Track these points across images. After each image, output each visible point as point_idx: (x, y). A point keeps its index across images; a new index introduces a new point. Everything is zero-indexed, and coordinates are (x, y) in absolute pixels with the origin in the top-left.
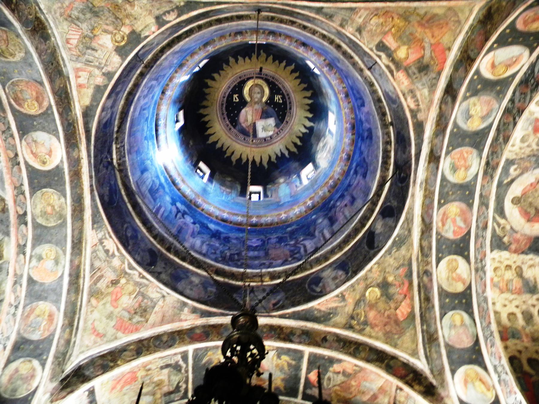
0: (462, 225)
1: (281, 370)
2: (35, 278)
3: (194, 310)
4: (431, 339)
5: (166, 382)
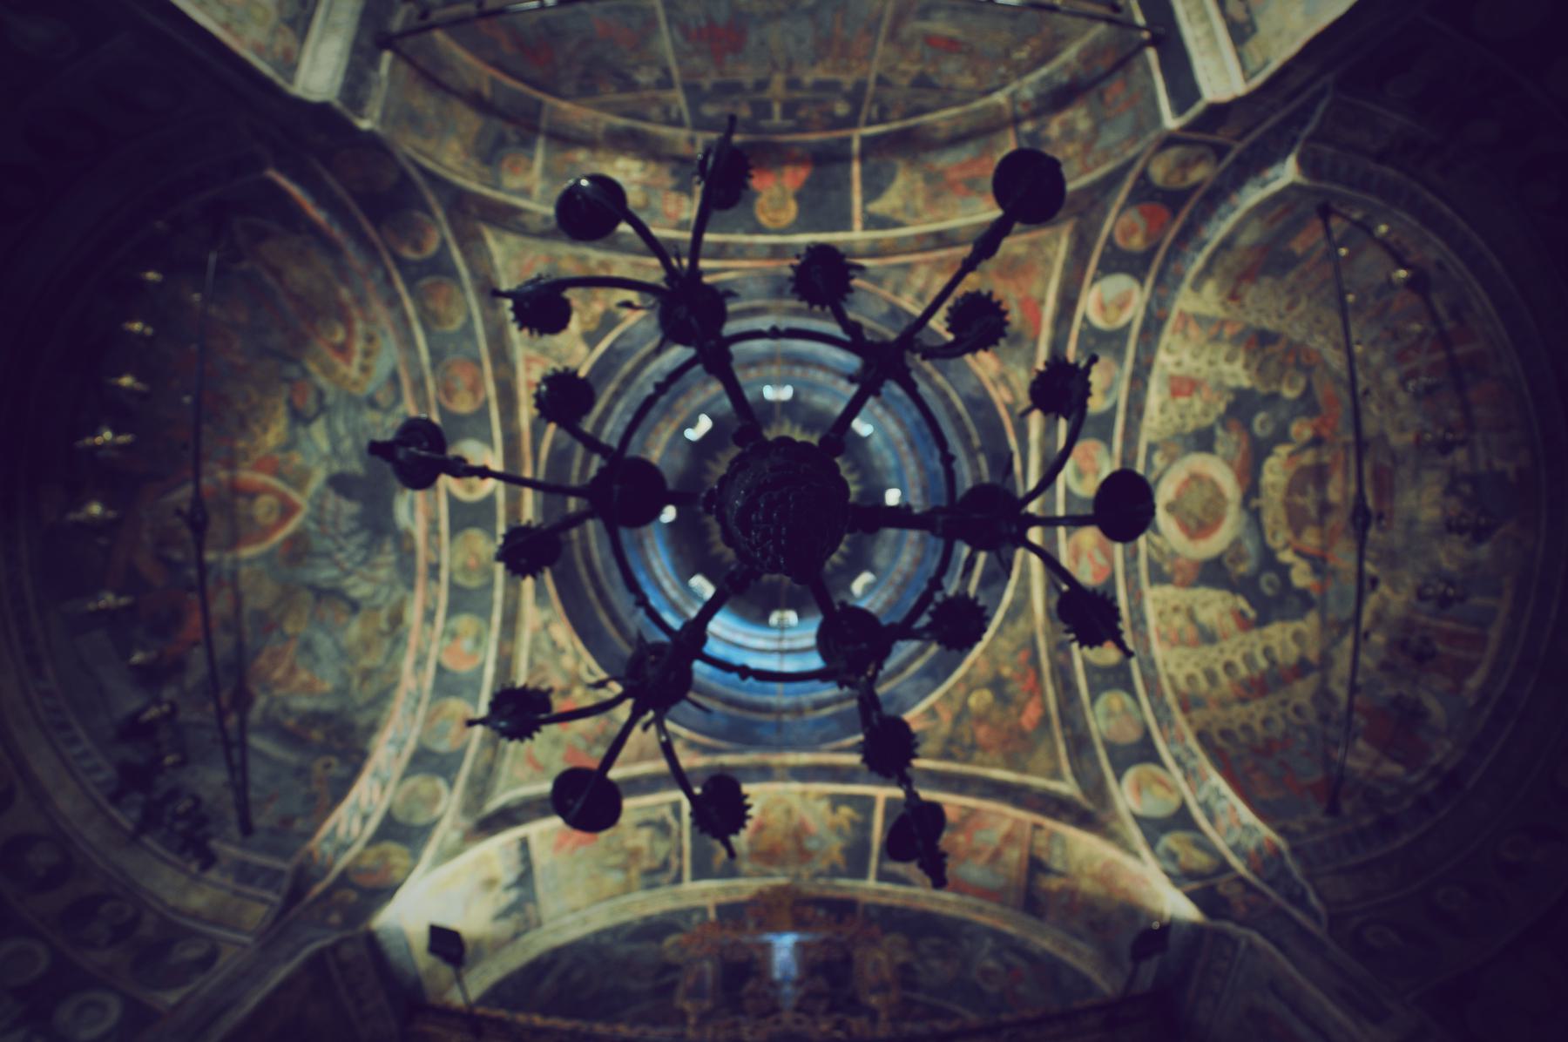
4: (1080, 744)
5: (646, 852)
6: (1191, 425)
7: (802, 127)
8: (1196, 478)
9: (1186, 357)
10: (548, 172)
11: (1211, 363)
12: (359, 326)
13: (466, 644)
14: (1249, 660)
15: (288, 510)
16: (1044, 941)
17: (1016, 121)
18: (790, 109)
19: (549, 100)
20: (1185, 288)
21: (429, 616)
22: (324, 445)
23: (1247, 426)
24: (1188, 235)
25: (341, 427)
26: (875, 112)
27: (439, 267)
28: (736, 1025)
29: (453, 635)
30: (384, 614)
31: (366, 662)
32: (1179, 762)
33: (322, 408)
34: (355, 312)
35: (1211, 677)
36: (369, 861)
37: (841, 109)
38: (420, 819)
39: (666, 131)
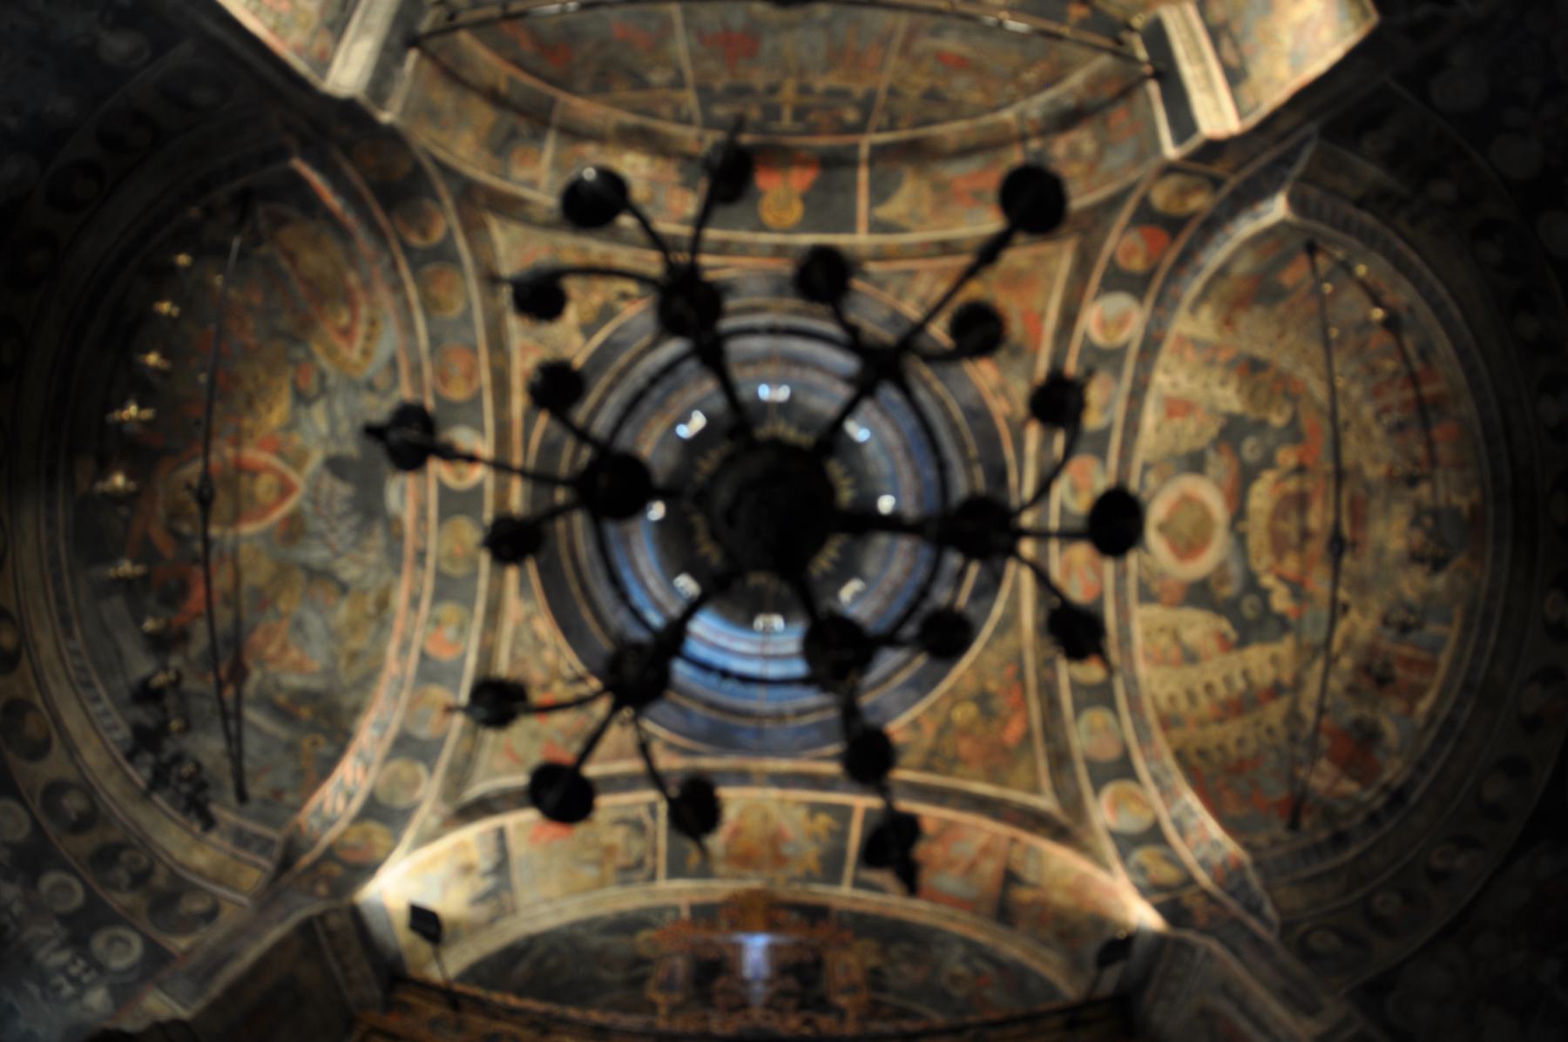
0: (1091, 577)
1: (815, 837)
2: (432, 650)
3: (670, 747)
4: (1060, 760)
6: (1184, 446)
7: (812, 131)
8: (1187, 501)
9: (1181, 377)
10: (557, 164)
11: (1206, 386)
12: (364, 311)
13: (449, 633)
14: (1228, 681)
15: (285, 489)
16: (1014, 948)
17: (1023, 138)
18: (800, 113)
19: (563, 97)
20: (1182, 312)
21: (415, 602)
22: (322, 426)
23: (1236, 449)
24: (1186, 259)
25: (340, 409)
26: (884, 121)
27: (444, 254)
28: (705, 1018)
29: (436, 622)
30: (371, 599)
31: (354, 644)
32: (1156, 779)
33: (324, 390)
34: (360, 297)
35: (1191, 697)
36: (353, 839)
37: (851, 116)
38: (401, 802)
39: (675, 130)
